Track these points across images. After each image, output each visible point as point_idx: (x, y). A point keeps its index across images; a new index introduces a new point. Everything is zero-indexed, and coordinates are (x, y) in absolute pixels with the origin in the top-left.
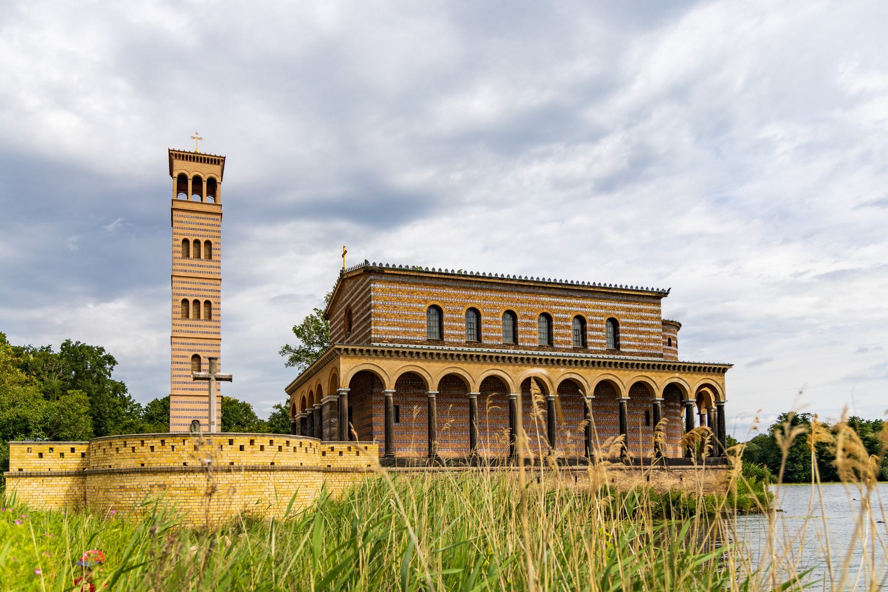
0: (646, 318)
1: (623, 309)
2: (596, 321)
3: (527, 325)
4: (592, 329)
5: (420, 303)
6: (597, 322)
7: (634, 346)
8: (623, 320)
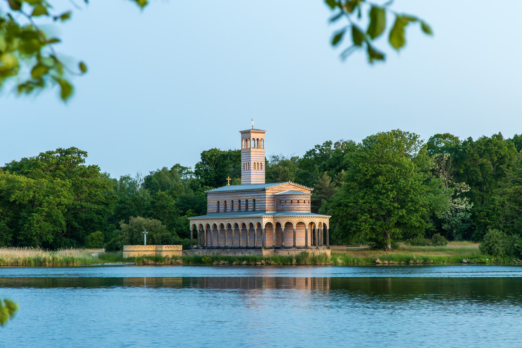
3: (236, 204)
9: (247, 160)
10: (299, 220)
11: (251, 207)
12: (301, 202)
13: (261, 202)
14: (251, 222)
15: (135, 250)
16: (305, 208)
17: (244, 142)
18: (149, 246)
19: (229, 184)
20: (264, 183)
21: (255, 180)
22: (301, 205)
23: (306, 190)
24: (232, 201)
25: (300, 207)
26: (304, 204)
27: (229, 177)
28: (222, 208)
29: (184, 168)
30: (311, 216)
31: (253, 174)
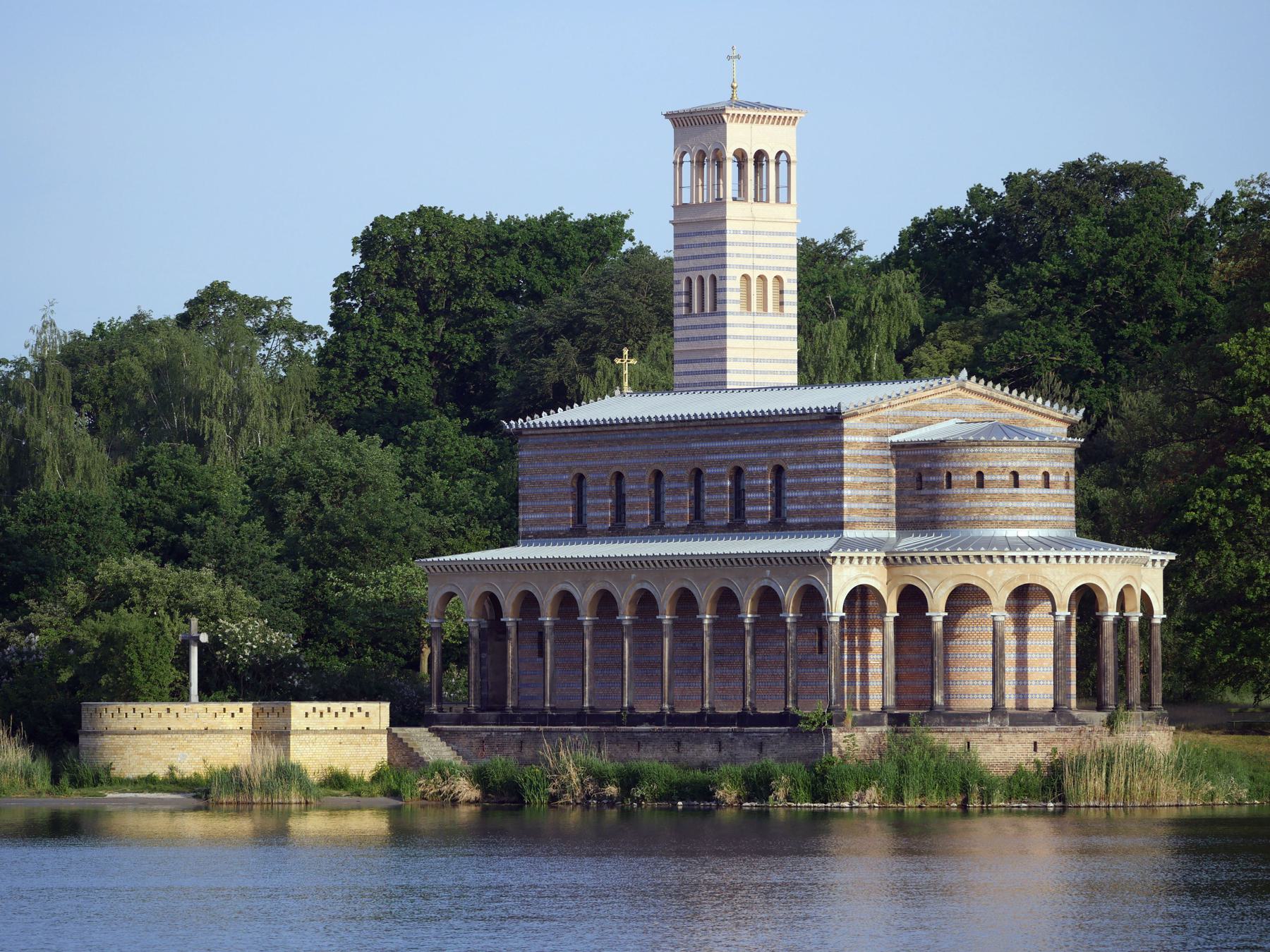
1: (792, 447)
3: (677, 491)
5: (564, 473)
9: (707, 262)
10: (1021, 577)
12: (1030, 483)
13: (817, 480)
14: (765, 583)
15: (146, 727)
16: (1049, 511)
17: (687, 167)
18: (214, 707)
19: (626, 384)
20: (794, 380)
21: (749, 366)
22: (1031, 497)
23: (1047, 421)
24: (658, 475)
25: (1024, 504)
26: (1046, 491)
27: (626, 352)
29: (258, 305)
30: (1082, 554)
31: (736, 337)
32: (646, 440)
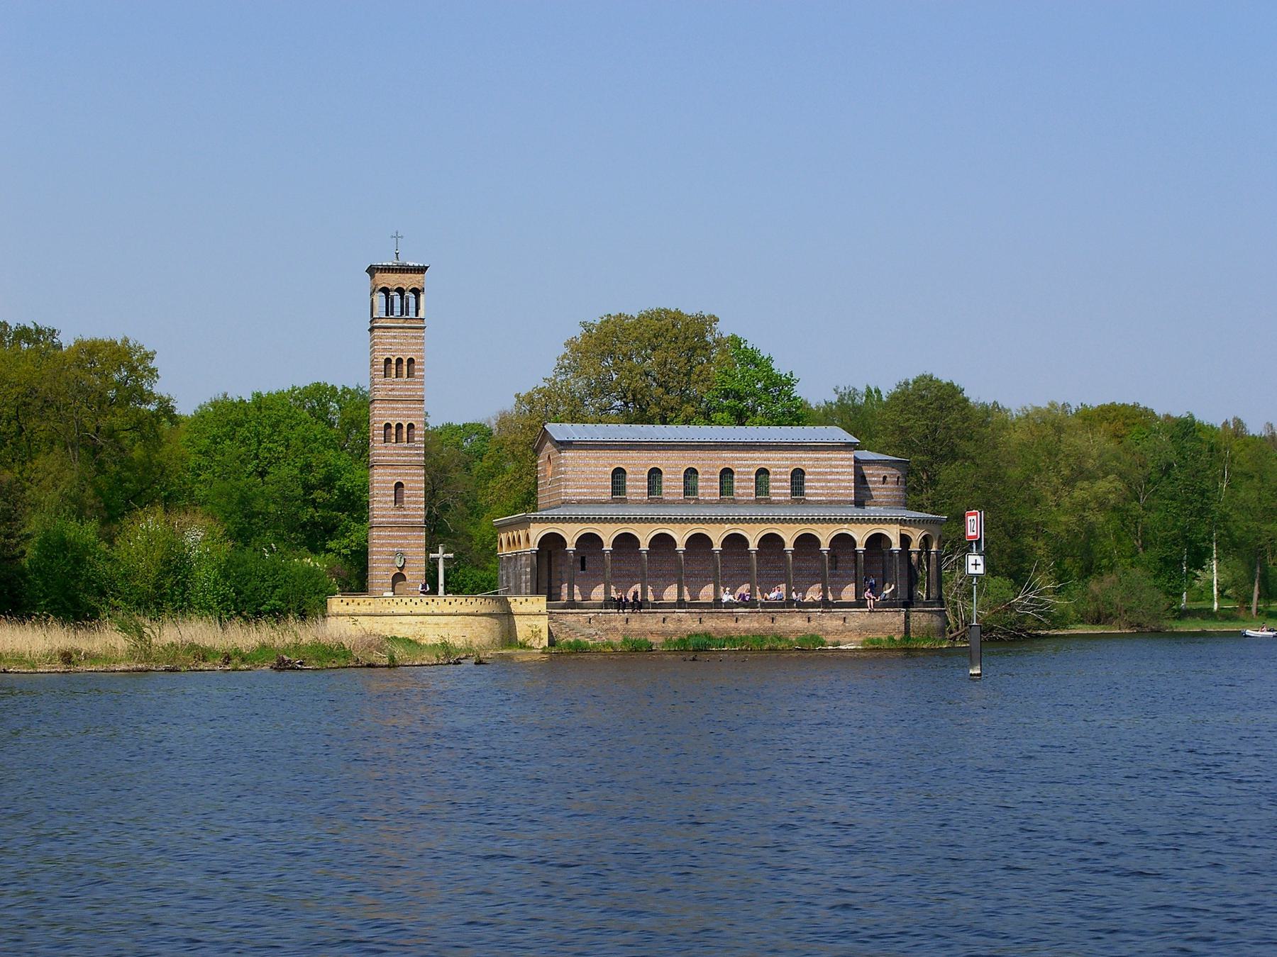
0: (836, 466)
1: (811, 459)
2: (781, 472)
3: (708, 480)
4: (776, 481)
6: (781, 473)
7: (822, 495)
8: (810, 470)
11: (780, 488)
28: (636, 486)
32: (681, 450)
